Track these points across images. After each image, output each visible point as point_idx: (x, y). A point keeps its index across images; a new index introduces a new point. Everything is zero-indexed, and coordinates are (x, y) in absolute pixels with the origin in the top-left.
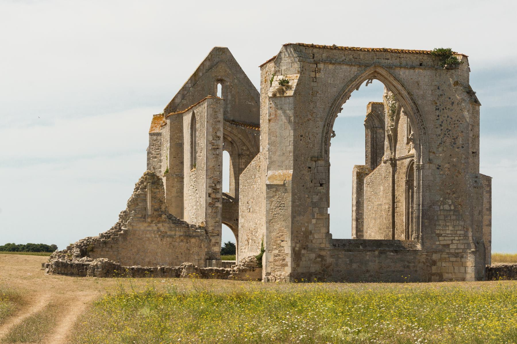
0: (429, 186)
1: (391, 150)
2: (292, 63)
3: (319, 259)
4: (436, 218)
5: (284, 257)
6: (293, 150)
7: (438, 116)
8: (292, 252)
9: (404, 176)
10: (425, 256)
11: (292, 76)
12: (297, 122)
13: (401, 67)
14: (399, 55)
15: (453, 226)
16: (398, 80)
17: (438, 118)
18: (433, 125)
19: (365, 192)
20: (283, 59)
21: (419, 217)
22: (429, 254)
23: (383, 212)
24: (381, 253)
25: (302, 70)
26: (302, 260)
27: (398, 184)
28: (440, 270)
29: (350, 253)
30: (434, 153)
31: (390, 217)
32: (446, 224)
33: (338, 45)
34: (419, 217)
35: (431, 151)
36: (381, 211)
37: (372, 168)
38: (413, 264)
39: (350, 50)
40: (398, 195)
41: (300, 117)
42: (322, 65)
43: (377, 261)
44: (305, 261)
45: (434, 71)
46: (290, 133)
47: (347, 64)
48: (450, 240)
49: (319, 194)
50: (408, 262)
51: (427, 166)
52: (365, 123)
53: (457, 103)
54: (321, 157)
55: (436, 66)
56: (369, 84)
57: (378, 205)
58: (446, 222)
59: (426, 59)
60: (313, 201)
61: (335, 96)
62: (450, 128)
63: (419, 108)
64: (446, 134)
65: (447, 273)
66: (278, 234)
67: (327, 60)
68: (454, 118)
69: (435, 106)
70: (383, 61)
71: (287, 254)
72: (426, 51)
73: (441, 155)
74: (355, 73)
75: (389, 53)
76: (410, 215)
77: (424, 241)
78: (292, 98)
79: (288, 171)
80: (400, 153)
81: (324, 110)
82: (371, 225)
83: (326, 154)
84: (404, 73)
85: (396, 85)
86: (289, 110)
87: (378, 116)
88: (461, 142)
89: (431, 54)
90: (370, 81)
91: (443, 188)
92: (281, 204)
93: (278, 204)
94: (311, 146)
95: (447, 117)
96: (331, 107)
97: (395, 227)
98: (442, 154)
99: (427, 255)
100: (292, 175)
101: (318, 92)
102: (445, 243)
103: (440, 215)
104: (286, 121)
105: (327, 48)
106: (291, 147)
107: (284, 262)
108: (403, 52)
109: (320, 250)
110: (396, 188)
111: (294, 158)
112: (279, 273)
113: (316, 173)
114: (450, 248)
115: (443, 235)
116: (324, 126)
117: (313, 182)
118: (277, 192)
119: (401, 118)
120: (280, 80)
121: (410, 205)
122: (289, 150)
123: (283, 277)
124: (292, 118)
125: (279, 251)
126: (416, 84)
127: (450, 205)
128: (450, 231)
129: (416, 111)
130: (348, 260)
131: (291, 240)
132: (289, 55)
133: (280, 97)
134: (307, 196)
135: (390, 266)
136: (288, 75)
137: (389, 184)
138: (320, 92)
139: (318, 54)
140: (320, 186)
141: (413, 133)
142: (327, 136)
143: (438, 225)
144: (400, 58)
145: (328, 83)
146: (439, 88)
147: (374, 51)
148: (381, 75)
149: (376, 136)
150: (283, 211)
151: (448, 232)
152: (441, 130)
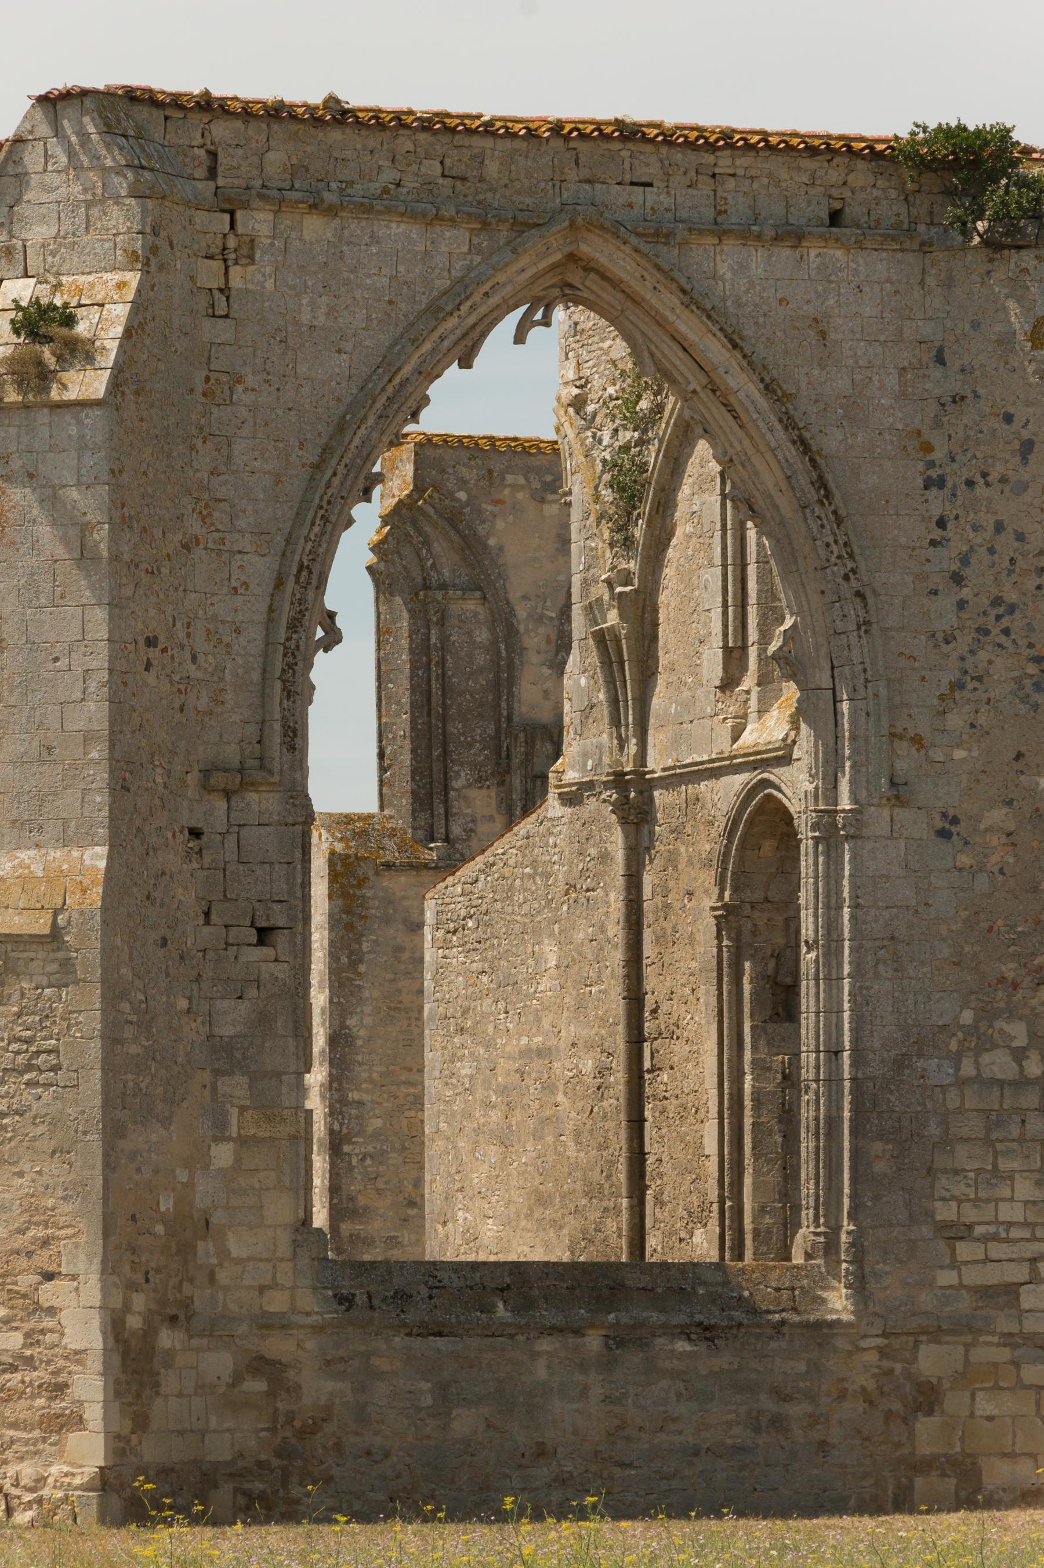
0: (892, 938)
1: (616, 721)
2: (89, 205)
3: (257, 1386)
4: (933, 1130)
5: (56, 1373)
6: (106, 725)
7: (941, 523)
8: (111, 1343)
9: (708, 878)
10: (872, 1357)
11: (92, 285)
12: (127, 557)
13: (721, 232)
14: (709, 158)
16: (704, 310)
17: (937, 534)
18: (909, 579)
19: (428, 976)
20: (34, 180)
21: (833, 1123)
22: (897, 1343)
23: (560, 1098)
24: (621, 1343)
25: (154, 250)
26: (163, 1390)
27: (668, 926)
28: (962, 1440)
29: (439, 1342)
30: (917, 741)
31: (610, 1124)
32: (995, 1166)
33: (355, 98)
34: (833, 1123)
36: (549, 1088)
37: (421, 834)
38: (806, 1407)
39: (424, 129)
40: (661, 993)
41: (144, 529)
42: (261, 216)
43: (597, 1391)
44: (180, 1395)
45: (910, 257)
46: (89, 626)
47: (410, 215)
48: (1020, 1260)
49: (252, 993)
50: (782, 1396)
51: (880, 818)
52: (370, 558)
54: (261, 767)
55: (922, 228)
56: (536, 334)
57: (526, 1053)
58: (996, 1154)
59: (863, 189)
60: (217, 1031)
61: (339, 400)
62: (1012, 596)
63: (829, 478)
64: (987, 633)
65: (1004, 1455)
66: (22, 1231)
67: (292, 188)
69: (921, 466)
70: (619, 195)
71: (77, 1352)
72: (862, 139)
73: (959, 754)
74: (458, 265)
75: (648, 148)
76: (748, 1112)
77: (867, 1270)
78: (98, 412)
79: (75, 854)
80: (676, 741)
81: (278, 482)
82: (477, 1178)
83: (292, 748)
84: (742, 267)
85: (692, 337)
86: (79, 483)
87: (453, 519)
89: (892, 159)
90: (538, 316)
91: (977, 948)
92: (38, 1053)
93: (18, 1053)
94: (204, 703)
95: (991, 528)
96: (318, 467)
97: (647, 1187)
98: (970, 750)
99: (882, 1352)
100: (101, 877)
101: (239, 380)
102: (990, 1276)
103: (960, 1110)
104: (60, 551)
105: (293, 117)
106: (92, 706)
107: (58, 1405)
108: (731, 146)
109: (261, 1327)
110: (649, 950)
111: (111, 772)
112: (27, 1471)
113: (230, 868)
114: (1025, 1305)
115: (979, 1230)
116: (279, 583)
117: (214, 917)
118: (12, 978)
119: (679, 532)
120: (18, 307)
121: (748, 1055)
122: (80, 725)
123: (60, 1494)
124: (101, 536)
125: (27, 1335)
126: (812, 333)
127: (1019, 1055)
128: (1018, 1207)
129: (812, 495)
130: (425, 1386)
131: (102, 1273)
132: (71, 154)
133: (26, 407)
134: (183, 1004)
135: (674, 1420)
136: (64, 279)
137: (603, 929)
138: (250, 380)
139: (240, 152)
141: (794, 626)
142: (292, 644)
143: (945, 1171)
145: (296, 322)
146: (940, 359)
147: (567, 138)
148: (604, 276)
149: (444, 639)
150: (47, 1095)
151: (1006, 1212)
152: (961, 605)
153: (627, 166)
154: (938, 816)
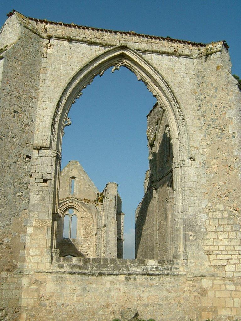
7: (200, 106)
15: (228, 240)
17: (199, 108)
35: (193, 145)
43: (122, 290)
49: (41, 193)
53: (221, 88)
68: (220, 105)
73: (205, 150)
88: (230, 131)
102: (218, 263)
127: (222, 212)
128: (224, 247)
135: (142, 297)
138: (50, 69)
140: (42, 182)
144: (151, 43)
152: (205, 121)
153: (133, 39)
154: (201, 163)
